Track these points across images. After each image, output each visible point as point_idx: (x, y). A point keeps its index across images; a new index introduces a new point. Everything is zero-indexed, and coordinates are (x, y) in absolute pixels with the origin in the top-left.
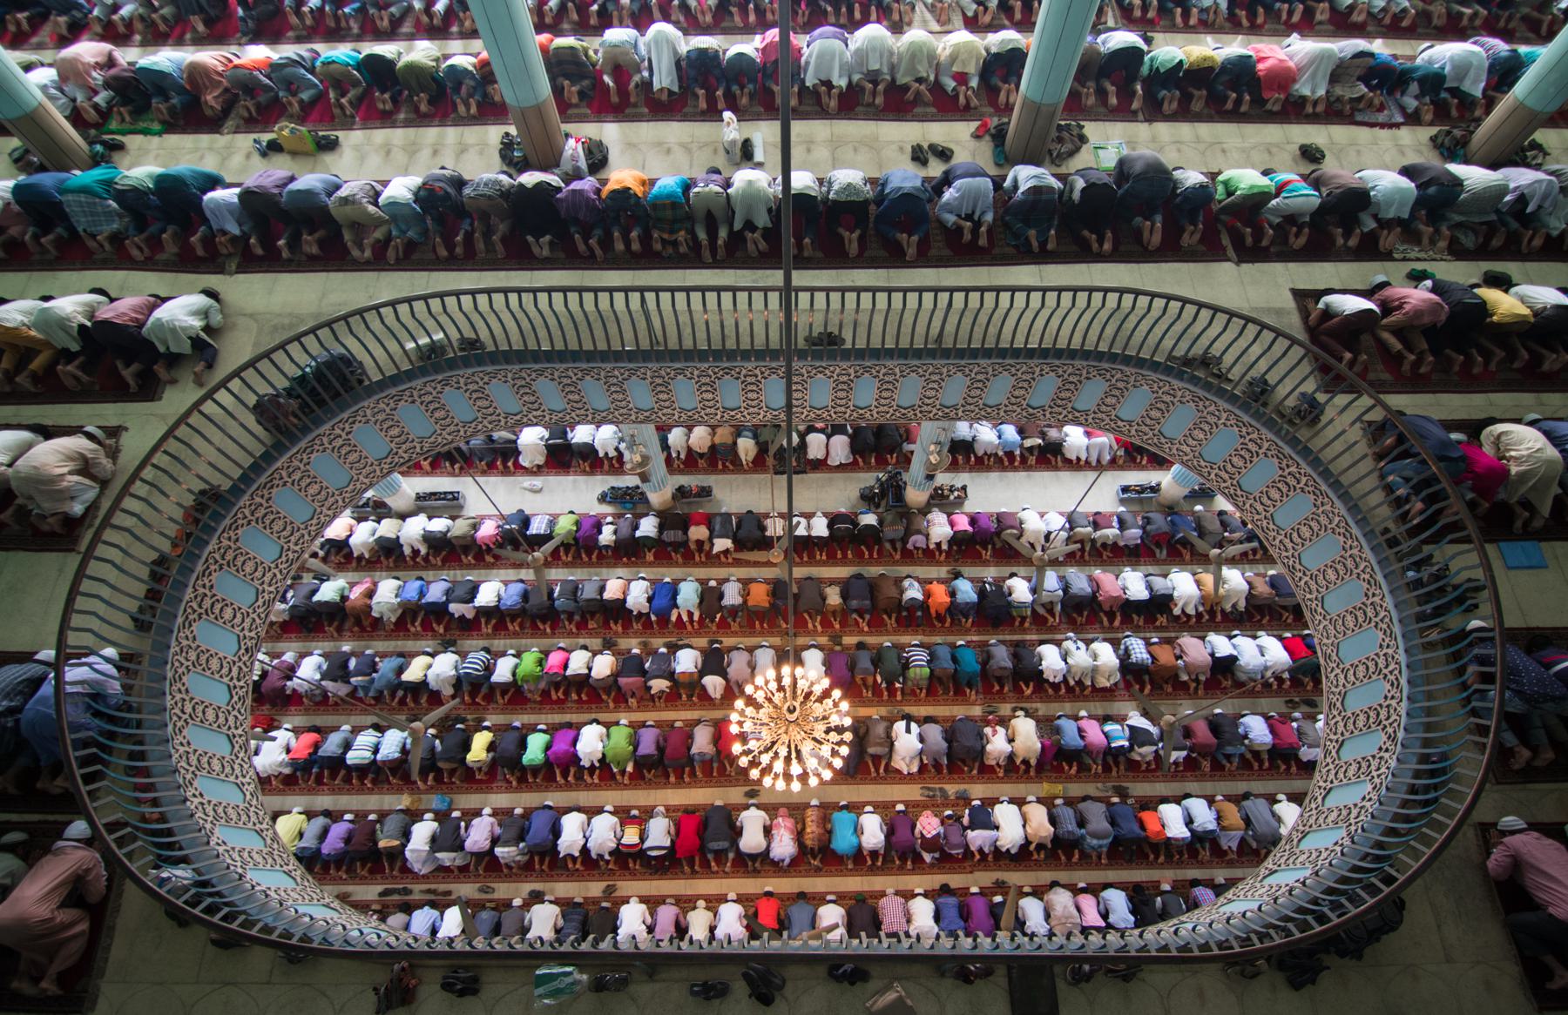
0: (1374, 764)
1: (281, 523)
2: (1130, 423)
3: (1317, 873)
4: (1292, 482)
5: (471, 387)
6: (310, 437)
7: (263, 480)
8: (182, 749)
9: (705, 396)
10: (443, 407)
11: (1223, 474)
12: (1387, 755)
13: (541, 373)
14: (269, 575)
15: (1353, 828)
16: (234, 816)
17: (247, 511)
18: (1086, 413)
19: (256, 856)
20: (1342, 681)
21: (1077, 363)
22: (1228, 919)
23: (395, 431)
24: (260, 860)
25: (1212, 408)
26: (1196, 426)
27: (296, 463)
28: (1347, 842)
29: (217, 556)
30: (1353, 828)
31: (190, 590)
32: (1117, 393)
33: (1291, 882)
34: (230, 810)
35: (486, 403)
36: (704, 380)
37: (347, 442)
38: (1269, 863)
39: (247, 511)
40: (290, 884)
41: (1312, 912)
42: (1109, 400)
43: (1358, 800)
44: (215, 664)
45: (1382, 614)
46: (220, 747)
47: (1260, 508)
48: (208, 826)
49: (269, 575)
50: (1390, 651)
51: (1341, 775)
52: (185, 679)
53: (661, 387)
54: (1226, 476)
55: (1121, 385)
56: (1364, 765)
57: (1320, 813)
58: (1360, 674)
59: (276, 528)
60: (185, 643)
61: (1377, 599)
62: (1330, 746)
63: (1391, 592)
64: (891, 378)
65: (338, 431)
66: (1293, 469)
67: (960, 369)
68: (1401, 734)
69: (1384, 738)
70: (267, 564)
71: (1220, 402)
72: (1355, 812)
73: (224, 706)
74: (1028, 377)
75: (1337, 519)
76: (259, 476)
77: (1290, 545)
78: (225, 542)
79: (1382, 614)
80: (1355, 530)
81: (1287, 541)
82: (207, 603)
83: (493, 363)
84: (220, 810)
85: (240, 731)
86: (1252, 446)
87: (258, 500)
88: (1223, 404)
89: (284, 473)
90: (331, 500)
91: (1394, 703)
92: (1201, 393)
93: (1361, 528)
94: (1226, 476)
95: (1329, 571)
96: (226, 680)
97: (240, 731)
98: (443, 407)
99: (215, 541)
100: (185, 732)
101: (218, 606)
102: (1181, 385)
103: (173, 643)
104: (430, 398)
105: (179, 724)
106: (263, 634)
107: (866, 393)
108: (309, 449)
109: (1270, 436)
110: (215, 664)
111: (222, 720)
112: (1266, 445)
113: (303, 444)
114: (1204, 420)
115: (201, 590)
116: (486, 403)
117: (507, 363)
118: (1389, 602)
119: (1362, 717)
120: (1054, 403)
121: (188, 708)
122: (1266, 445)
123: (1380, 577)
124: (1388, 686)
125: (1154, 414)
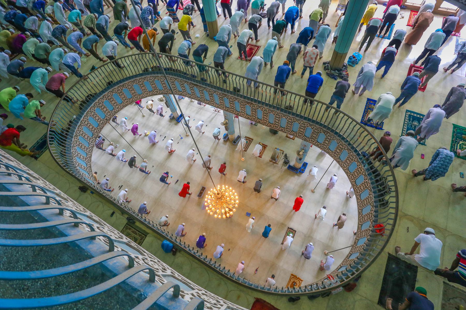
6: (134, 79)
14: (117, 106)
19: (81, 156)
24: (82, 158)
31: (97, 100)
37: (142, 84)
40: (85, 165)
44: (97, 118)
46: (90, 134)
73: (95, 127)
82: (101, 105)
84: (80, 145)
103: (89, 109)
104: (162, 80)
110: (97, 118)
111: (93, 129)
121: (86, 123)
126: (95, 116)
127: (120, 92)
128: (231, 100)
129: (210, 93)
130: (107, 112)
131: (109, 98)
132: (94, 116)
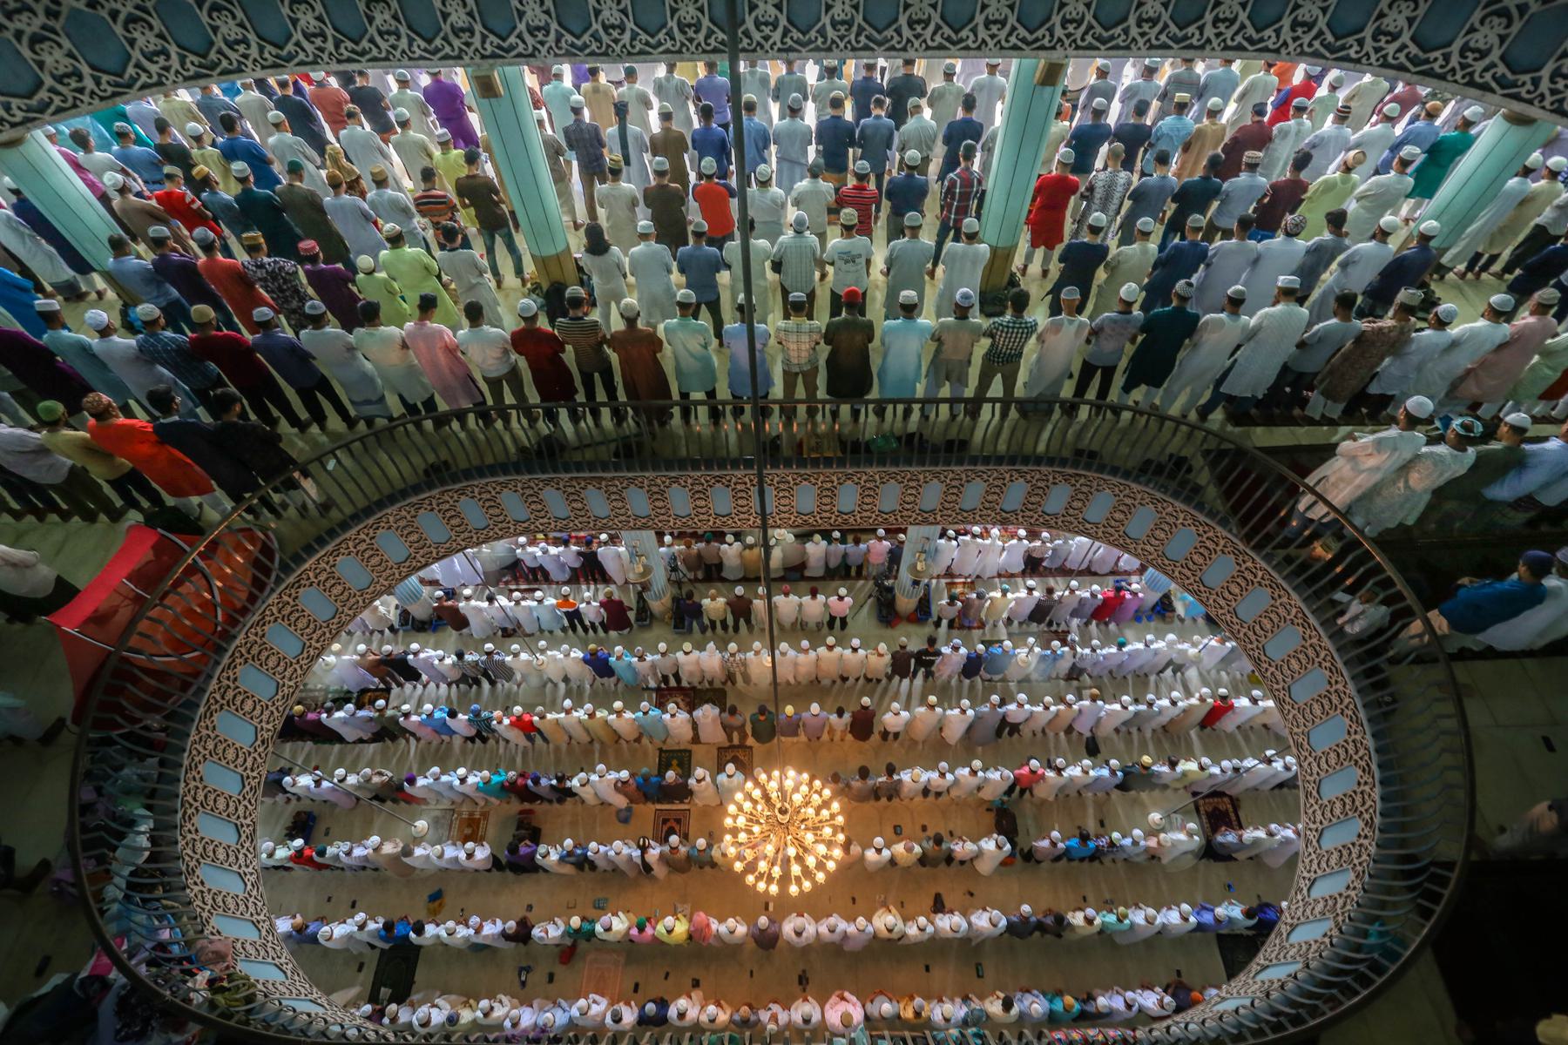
0: (1355, 851)
1: (305, 621)
2: (1096, 525)
3: (1307, 966)
4: (1250, 577)
5: (485, 496)
7: (291, 579)
8: (189, 836)
9: (699, 503)
10: (458, 515)
11: (1185, 571)
12: (1366, 842)
13: (547, 482)
14: (290, 670)
15: (1340, 919)
16: (232, 907)
17: (275, 610)
18: (1055, 515)
19: (248, 946)
20: (1315, 769)
21: (1044, 469)
22: (1221, 1018)
23: (414, 537)
24: (253, 951)
25: (1170, 509)
26: (1157, 527)
27: (323, 565)
28: (1335, 932)
29: (243, 650)
30: (1340, 919)
31: (215, 681)
32: (1080, 496)
33: (1283, 976)
34: (229, 900)
35: (497, 511)
36: (697, 488)
38: (1260, 959)
39: (275, 610)
40: (281, 977)
41: (1302, 1005)
42: (1076, 504)
43: (1343, 890)
44: (231, 754)
45: (1347, 700)
46: (227, 836)
47: (1222, 602)
48: (205, 915)
49: (290, 670)
50: (1358, 737)
51: (1324, 865)
52: (200, 768)
53: (657, 495)
54: (1189, 573)
55: (1085, 489)
56: (1345, 853)
57: (1306, 904)
58: (1333, 762)
59: (300, 625)
60: (204, 732)
61: (1340, 686)
62: (1311, 835)
63: (1353, 678)
64: (871, 485)
65: (363, 536)
66: (1249, 564)
67: (936, 475)
68: (1377, 820)
69: (1362, 824)
70: (290, 658)
71: (1177, 504)
72: (1340, 902)
74: (999, 483)
75: (1294, 611)
76: (288, 575)
77: (1253, 638)
78: (252, 638)
79: (1347, 700)
80: (1312, 620)
81: (1251, 634)
82: (230, 694)
83: (505, 473)
84: (219, 899)
85: (248, 821)
86: (1209, 544)
87: (286, 598)
88: (1179, 505)
89: (311, 574)
90: (353, 600)
91: (1367, 788)
92: (1159, 495)
93: (1318, 618)
94: (1189, 573)
95: (1293, 661)
96: (240, 770)
97: (248, 821)
98: (458, 515)
99: (242, 635)
100: (194, 820)
101: (240, 698)
102: (1140, 488)
103: (193, 732)
105: (189, 812)
106: (279, 727)
107: (848, 498)
108: (336, 553)
109: (1225, 533)
110: (231, 754)
111: (232, 809)
112: (1222, 542)
113: (330, 548)
114: (1163, 520)
115: (226, 682)
116: (497, 511)
117: (518, 472)
118: (1351, 688)
119: (1338, 805)
120: (1027, 506)
121: (201, 797)
122: (1222, 542)
123: (1340, 665)
124: (1360, 772)
125: (1118, 516)
126: (221, 748)
127: (289, 609)
128: (739, 487)
129: (655, 489)
130: (257, 712)
131: (255, 651)
132: (220, 750)
